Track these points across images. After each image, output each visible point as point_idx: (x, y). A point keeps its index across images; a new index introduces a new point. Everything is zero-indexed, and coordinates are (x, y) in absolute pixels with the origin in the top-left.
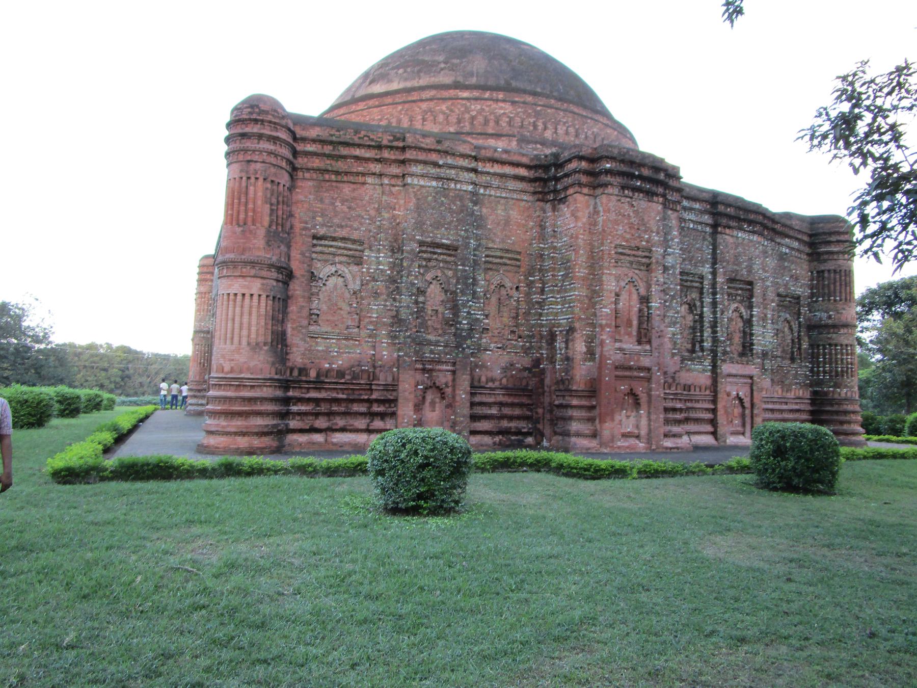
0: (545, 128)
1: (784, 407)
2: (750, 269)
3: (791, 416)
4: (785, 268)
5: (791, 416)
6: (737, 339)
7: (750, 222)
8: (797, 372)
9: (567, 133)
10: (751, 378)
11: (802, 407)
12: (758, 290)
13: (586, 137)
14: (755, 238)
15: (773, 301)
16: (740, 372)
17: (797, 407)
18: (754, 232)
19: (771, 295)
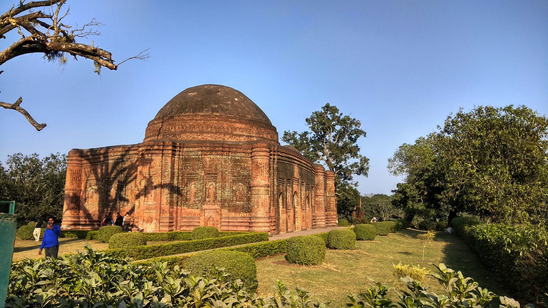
0: (172, 128)
1: (235, 221)
2: (216, 170)
3: (239, 224)
4: (237, 165)
5: (239, 224)
6: (212, 195)
7: (216, 151)
8: (243, 206)
9: (179, 128)
10: (215, 209)
11: (246, 220)
12: (219, 176)
13: (186, 127)
14: (218, 156)
15: (230, 179)
16: (211, 208)
17: (241, 221)
18: (217, 155)
19: (229, 177)
